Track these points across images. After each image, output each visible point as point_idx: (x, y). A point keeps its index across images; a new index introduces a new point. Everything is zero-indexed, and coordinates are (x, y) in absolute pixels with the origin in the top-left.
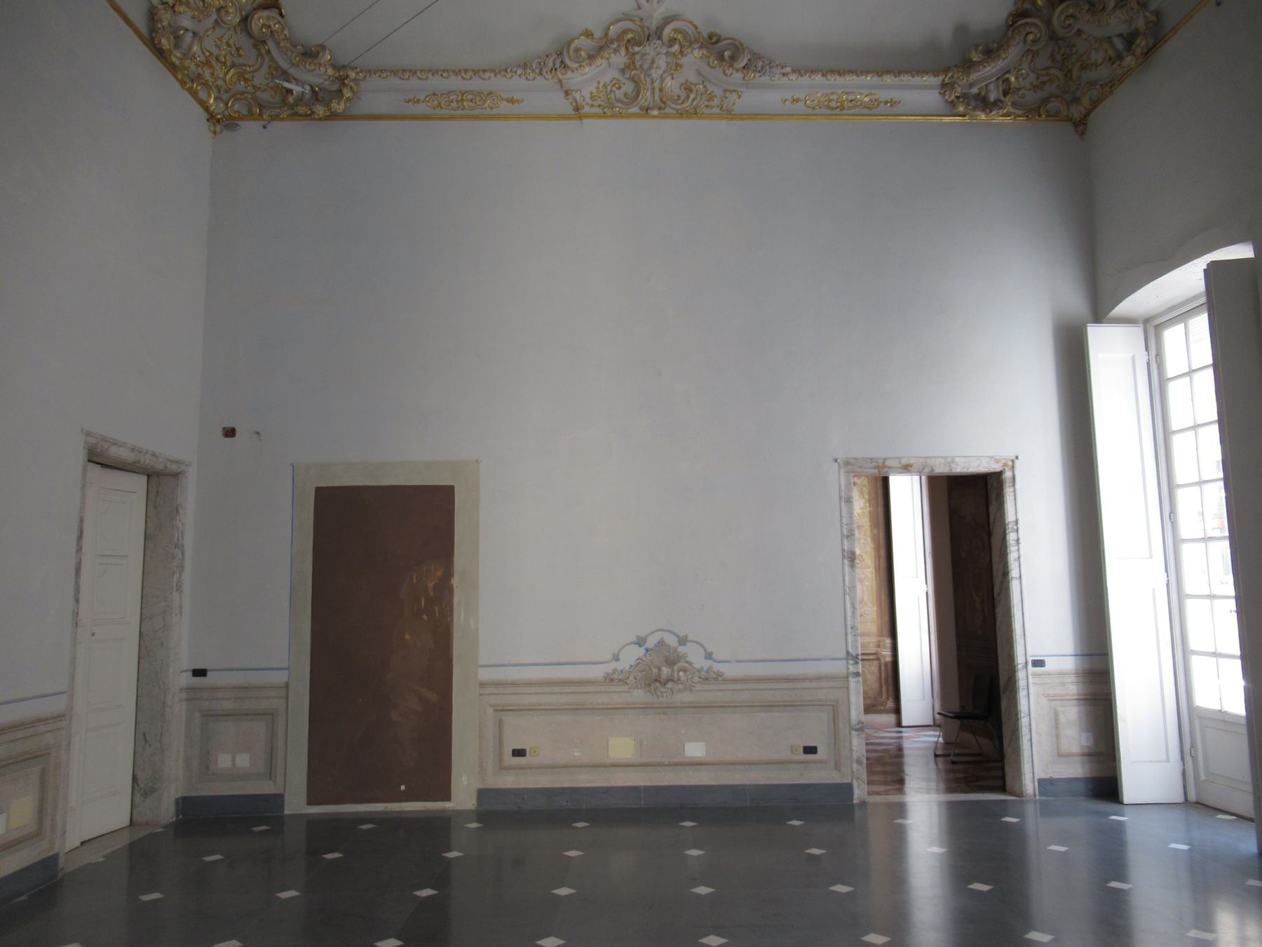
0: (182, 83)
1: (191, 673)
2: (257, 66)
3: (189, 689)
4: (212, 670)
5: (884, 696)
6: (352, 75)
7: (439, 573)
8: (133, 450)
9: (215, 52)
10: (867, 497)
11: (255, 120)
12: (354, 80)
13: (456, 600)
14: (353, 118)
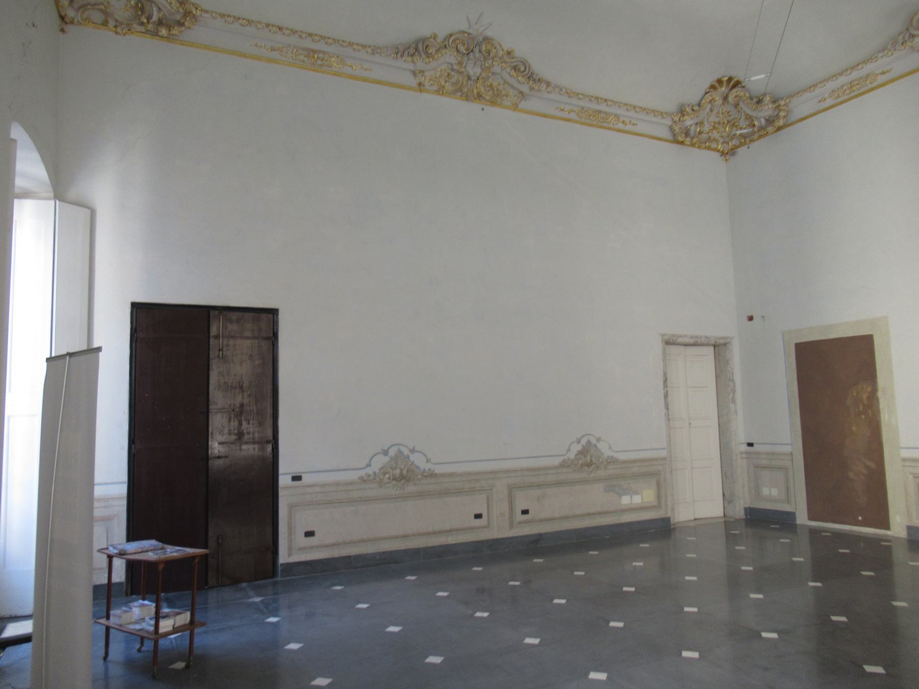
0: (699, 147)
1: (746, 445)
2: (739, 117)
3: (746, 453)
4: (756, 443)
6: (782, 103)
7: (869, 389)
8: (692, 337)
9: (717, 120)
11: (743, 146)
12: (784, 105)
13: (881, 406)
14: (791, 124)
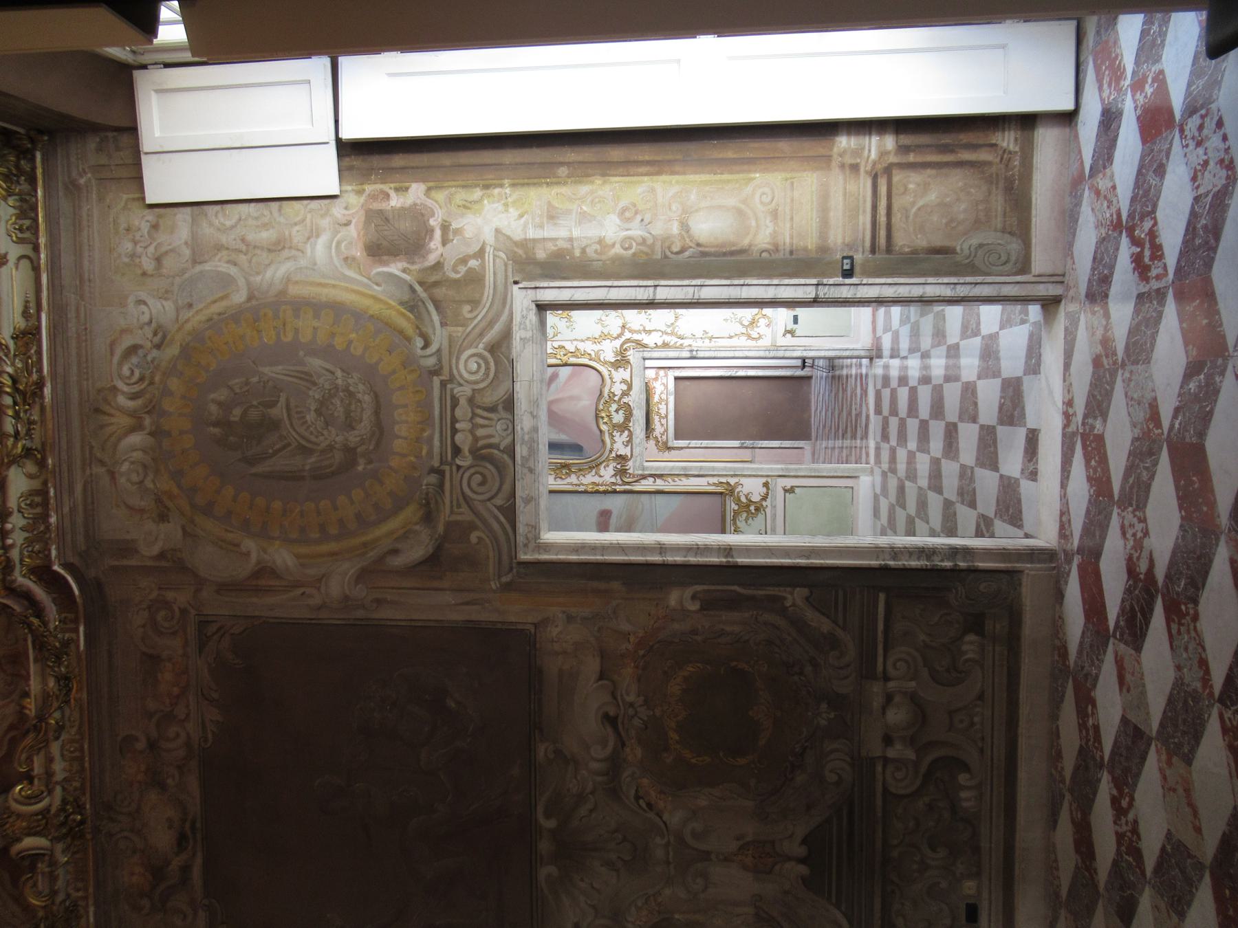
5: (983, 156)
10: (477, 193)
